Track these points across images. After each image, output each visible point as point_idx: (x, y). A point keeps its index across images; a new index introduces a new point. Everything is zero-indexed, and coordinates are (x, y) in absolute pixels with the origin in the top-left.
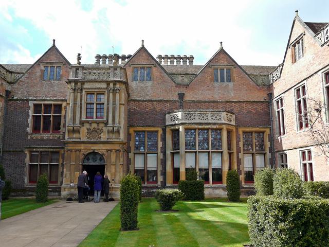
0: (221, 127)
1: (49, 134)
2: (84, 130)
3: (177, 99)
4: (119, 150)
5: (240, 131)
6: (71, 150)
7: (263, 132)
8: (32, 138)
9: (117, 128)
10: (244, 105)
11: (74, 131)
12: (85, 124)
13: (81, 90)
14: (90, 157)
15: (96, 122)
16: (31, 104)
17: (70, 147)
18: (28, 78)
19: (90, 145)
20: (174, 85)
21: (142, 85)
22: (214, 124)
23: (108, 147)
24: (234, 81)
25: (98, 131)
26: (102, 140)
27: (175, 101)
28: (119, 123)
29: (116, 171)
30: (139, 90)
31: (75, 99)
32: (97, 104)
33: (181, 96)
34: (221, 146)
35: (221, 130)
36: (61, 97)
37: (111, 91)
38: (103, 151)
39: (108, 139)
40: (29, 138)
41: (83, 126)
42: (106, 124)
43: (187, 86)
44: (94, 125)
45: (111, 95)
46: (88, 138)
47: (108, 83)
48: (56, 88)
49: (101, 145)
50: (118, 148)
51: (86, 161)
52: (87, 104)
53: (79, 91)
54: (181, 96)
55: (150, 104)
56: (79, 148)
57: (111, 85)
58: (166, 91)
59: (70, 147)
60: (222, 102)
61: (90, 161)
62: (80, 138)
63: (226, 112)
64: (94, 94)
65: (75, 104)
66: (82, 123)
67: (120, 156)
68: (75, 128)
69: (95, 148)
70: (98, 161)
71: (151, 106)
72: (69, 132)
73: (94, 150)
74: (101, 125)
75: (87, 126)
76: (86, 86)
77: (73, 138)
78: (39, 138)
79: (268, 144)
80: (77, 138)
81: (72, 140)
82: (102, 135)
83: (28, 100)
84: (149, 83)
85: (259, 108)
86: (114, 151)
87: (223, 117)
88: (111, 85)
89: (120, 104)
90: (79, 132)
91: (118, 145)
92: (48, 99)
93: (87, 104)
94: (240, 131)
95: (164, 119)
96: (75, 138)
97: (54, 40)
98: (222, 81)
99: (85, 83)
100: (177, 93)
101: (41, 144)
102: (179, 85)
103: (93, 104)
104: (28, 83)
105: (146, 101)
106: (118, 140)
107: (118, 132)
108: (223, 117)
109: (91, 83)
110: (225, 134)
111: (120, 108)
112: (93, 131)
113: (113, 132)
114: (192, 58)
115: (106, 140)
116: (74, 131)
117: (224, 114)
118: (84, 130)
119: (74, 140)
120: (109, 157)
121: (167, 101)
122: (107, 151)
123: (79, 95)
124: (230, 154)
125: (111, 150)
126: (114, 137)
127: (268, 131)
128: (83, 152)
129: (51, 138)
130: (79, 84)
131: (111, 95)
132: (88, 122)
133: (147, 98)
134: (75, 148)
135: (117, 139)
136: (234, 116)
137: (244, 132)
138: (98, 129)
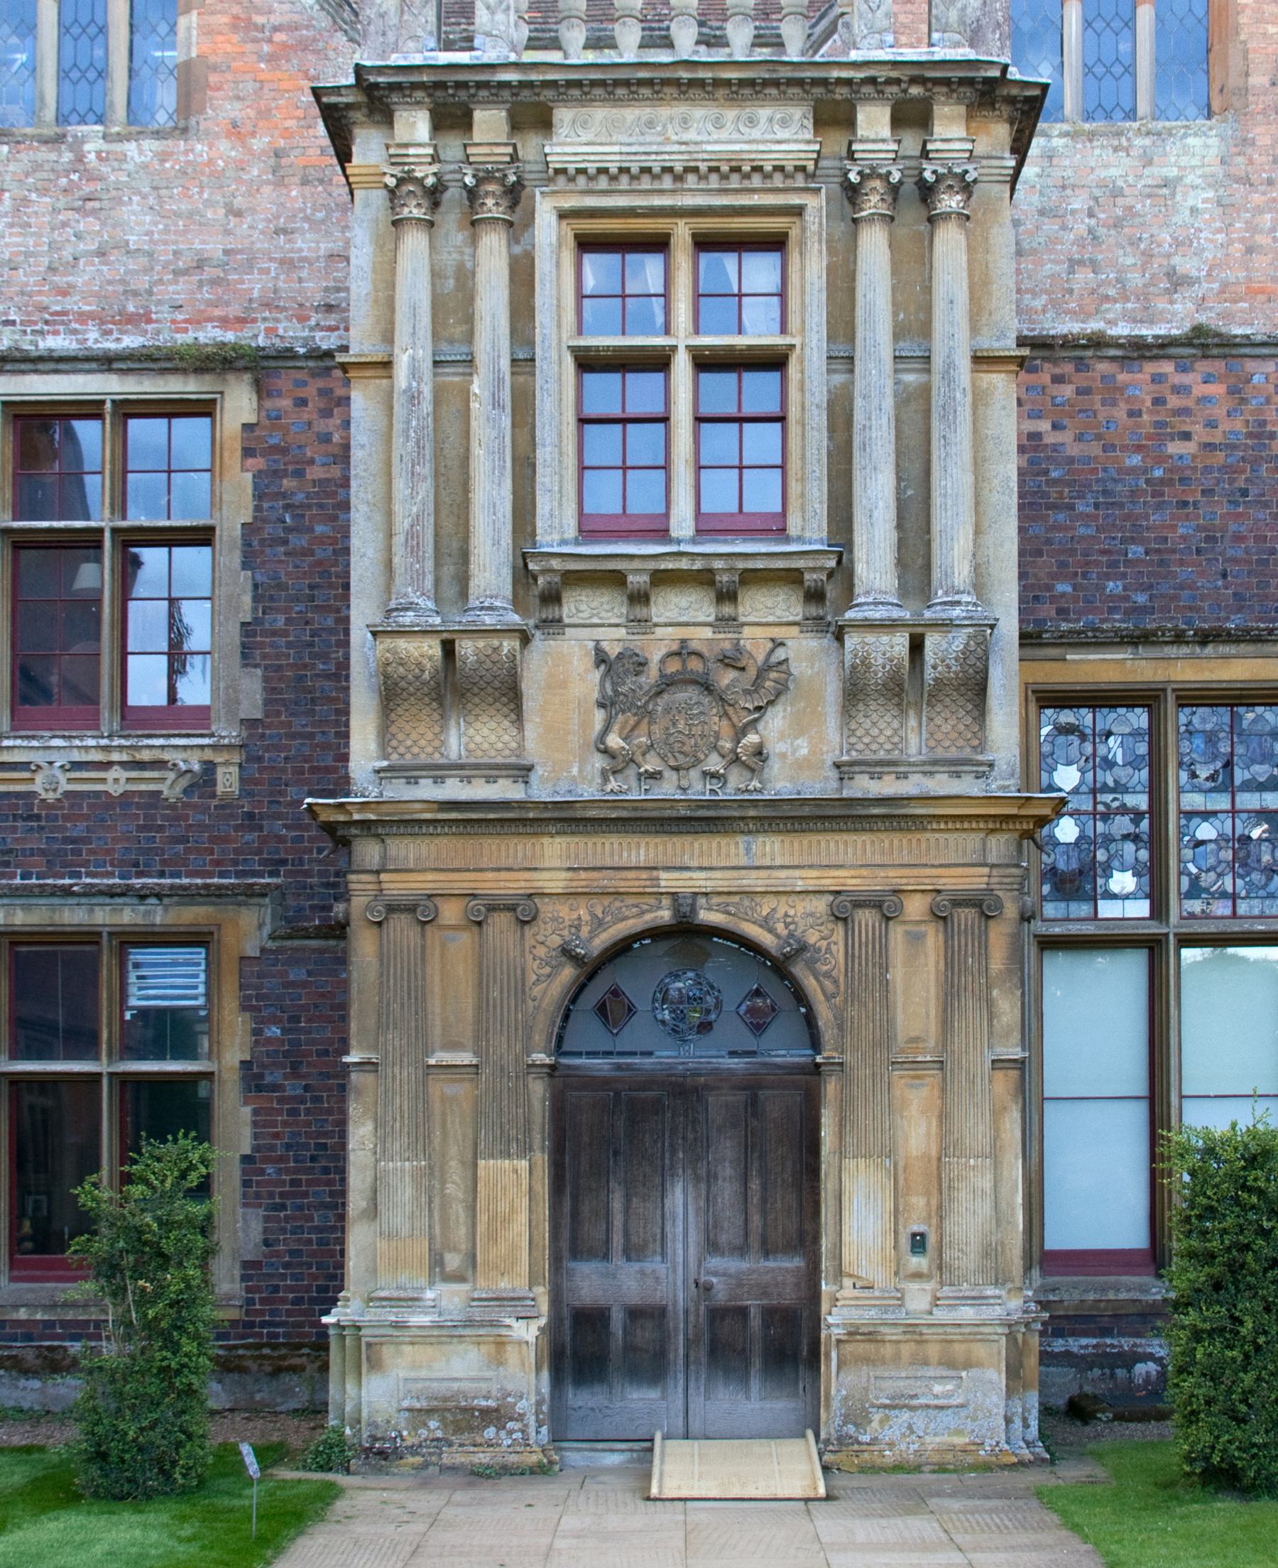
1: (88, 746)
2: (563, 672)
4: (982, 906)
6: (419, 911)
9: (958, 641)
12: (580, 606)
13: (515, 194)
14: (637, 983)
15: (704, 578)
17: (414, 868)
19: (640, 849)
23: (852, 861)
25: (722, 685)
26: (780, 783)
28: (979, 586)
29: (947, 1146)
30: (1081, 227)
31: (454, 305)
32: (706, 362)
36: (198, 321)
37: (873, 203)
38: (802, 907)
39: (844, 770)
41: (553, 625)
42: (815, 596)
44: (683, 615)
45: (874, 247)
46: (617, 763)
48: (137, 221)
49: (771, 847)
50: (974, 880)
51: (587, 1031)
52: (588, 362)
53: (492, 207)
55: (1202, 383)
56: (512, 884)
57: (874, 122)
59: (414, 868)
61: (639, 1033)
62: (523, 772)
64: (659, 244)
65: (453, 362)
66: (543, 590)
67: (997, 962)
68: (467, 649)
69: (705, 873)
70: (731, 1031)
71: (1219, 412)
72: (392, 694)
73: (683, 904)
74: (769, 610)
75: (595, 618)
76: (582, 136)
77: (439, 771)
80: (491, 771)
81: (427, 790)
82: (775, 724)
84: (1196, 150)
86: (915, 907)
89: (981, 360)
90: (508, 693)
91: (965, 844)
93: (588, 362)
96: (465, 770)
99: (563, 115)
103: (658, 362)
105: (1162, 348)
106: (968, 786)
107: (975, 689)
109: (631, 114)
111: (980, 399)
112: (668, 683)
113: (906, 686)
115: (821, 785)
116: (464, 682)
118: (563, 672)
119: (454, 790)
120: (870, 976)
122: (844, 908)
123: (493, 253)
125: (885, 906)
126: (914, 746)
128: (566, 922)
129: (116, 782)
130: (489, 122)
131: (874, 247)
133: (1175, 319)
134: (463, 883)
135: (955, 766)
138: (730, 661)
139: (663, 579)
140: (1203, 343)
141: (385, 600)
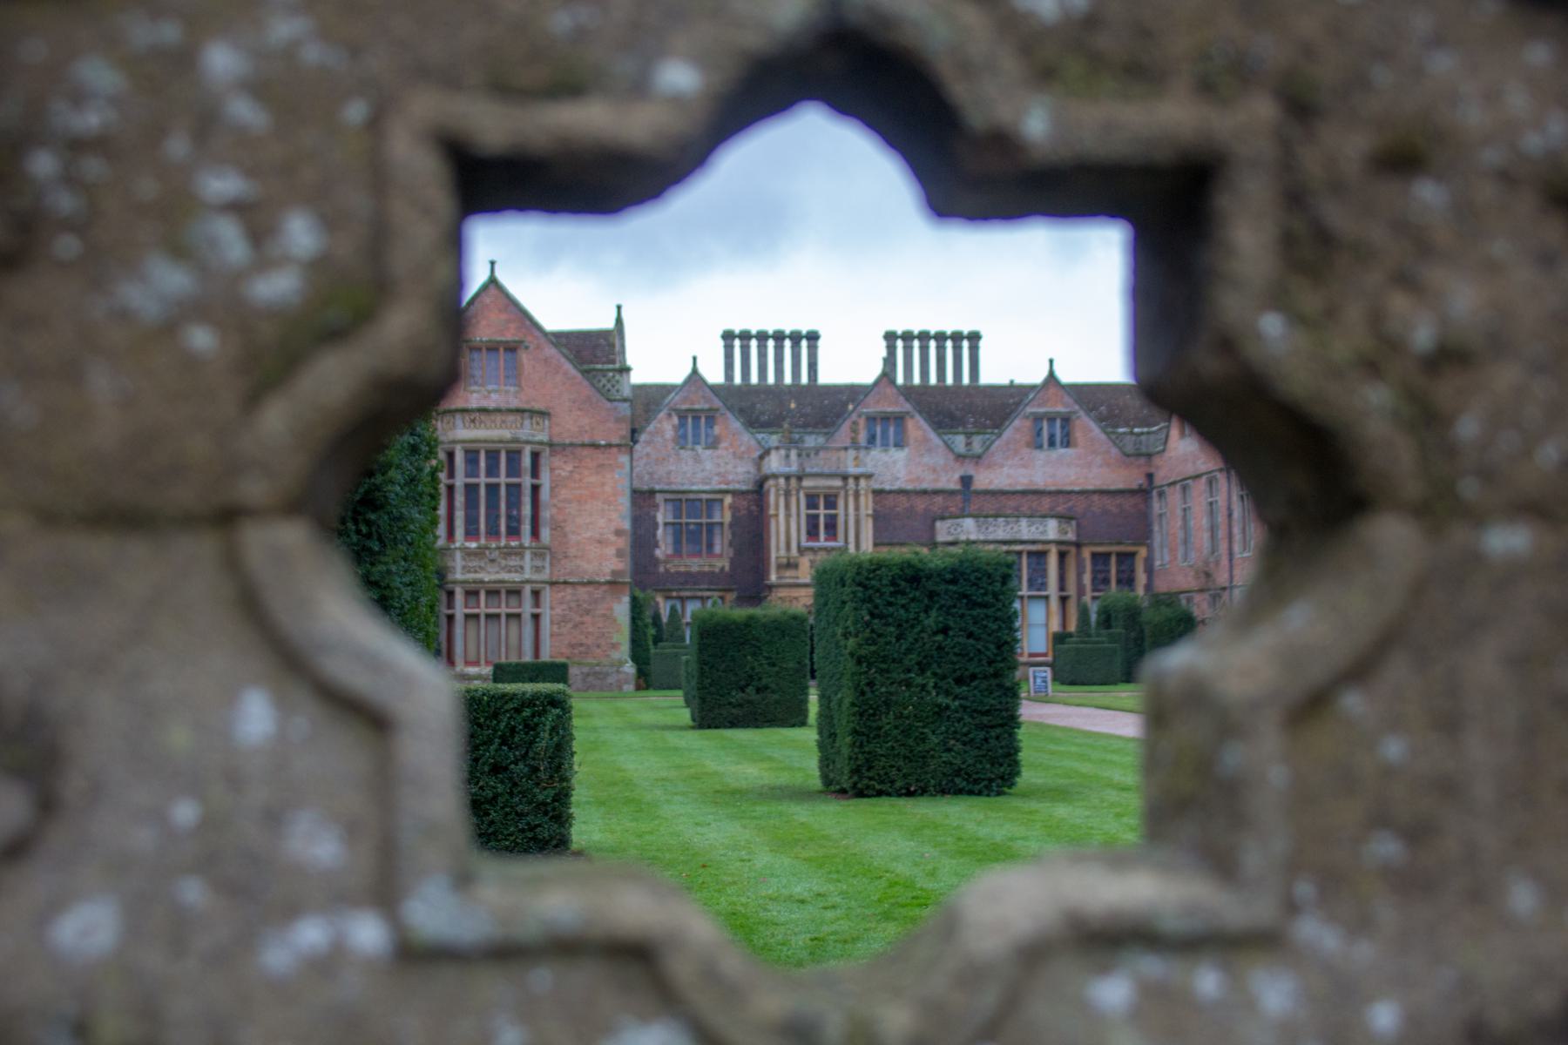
0: (1046, 547)
2: (805, 562)
3: (958, 487)
5: (1086, 553)
7: (1132, 555)
8: (667, 571)
10: (1096, 498)
11: (791, 565)
15: (825, 549)
16: (659, 498)
17: (783, 593)
18: (648, 443)
20: (951, 457)
21: (884, 457)
22: (1034, 542)
24: (1075, 446)
27: (952, 493)
33: (966, 481)
34: (1044, 586)
35: (1042, 555)
40: (662, 569)
43: (978, 458)
47: (845, 478)
48: (709, 466)
54: (966, 481)
55: (903, 499)
57: (851, 481)
58: (934, 470)
60: (1050, 493)
63: (1059, 517)
72: (779, 567)
76: (806, 483)
78: (682, 569)
79: (1141, 578)
83: (652, 492)
84: (899, 455)
85: (1128, 503)
88: (851, 481)
90: (795, 566)
92: (694, 488)
94: (1086, 553)
97: (695, 359)
98: (1052, 444)
100: (957, 476)
101: (686, 582)
102: (960, 457)
104: (648, 455)
114: (974, 337)
116: (791, 565)
118: (805, 562)
121: (936, 492)
124: (1064, 600)
127: (1143, 552)
129: (706, 569)
130: (793, 482)
132: (811, 549)
136: (1074, 523)
137: (1094, 555)
139: (821, 549)
140: (902, 492)
141: (776, 551)
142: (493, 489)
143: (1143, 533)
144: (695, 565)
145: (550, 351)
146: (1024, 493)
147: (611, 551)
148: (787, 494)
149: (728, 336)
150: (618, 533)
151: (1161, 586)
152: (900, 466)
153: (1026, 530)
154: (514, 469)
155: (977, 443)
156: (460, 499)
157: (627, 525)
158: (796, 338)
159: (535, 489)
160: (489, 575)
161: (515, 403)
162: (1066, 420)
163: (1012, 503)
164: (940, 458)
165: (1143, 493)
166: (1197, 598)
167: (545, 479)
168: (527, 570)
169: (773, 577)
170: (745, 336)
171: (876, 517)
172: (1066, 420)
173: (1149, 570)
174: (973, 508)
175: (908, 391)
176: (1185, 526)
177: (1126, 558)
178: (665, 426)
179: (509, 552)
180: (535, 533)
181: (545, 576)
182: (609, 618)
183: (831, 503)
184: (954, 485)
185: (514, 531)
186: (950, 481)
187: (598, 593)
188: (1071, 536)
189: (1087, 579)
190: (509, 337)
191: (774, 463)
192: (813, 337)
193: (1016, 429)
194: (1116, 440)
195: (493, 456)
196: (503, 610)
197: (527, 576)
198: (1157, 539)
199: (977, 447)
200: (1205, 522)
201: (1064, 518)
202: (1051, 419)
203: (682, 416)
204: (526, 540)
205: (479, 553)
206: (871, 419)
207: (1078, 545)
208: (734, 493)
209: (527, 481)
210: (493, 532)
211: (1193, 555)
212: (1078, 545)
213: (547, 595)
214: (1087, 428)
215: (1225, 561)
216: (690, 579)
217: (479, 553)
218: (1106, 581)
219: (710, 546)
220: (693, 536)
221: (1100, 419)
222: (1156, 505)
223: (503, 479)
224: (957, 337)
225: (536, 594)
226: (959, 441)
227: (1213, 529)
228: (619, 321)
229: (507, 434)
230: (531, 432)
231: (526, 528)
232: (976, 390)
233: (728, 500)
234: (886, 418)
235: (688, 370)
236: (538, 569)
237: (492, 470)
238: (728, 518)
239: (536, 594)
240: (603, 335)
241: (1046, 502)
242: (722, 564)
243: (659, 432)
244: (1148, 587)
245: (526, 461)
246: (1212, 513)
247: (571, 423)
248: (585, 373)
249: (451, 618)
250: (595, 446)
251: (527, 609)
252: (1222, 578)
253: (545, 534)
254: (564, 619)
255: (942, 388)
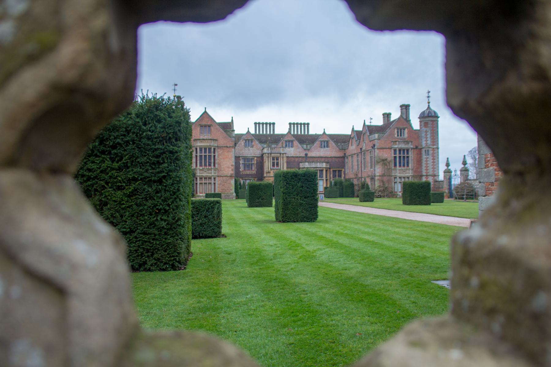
2: (272, 172)
5: (331, 170)
11: (269, 172)
16: (241, 158)
17: (267, 178)
33: (306, 155)
34: (322, 177)
35: (322, 170)
43: (309, 150)
47: (280, 154)
54: (306, 155)
63: (326, 162)
72: (266, 173)
76: (272, 155)
79: (343, 175)
83: (239, 157)
84: (292, 149)
85: (340, 160)
87: (324, 165)
90: (270, 173)
94: (331, 170)
95: (299, 165)
98: (324, 147)
102: (305, 150)
108: (324, 165)
110: (324, 172)
114: (308, 124)
116: (269, 172)
117: (324, 164)
118: (272, 172)
121: (300, 157)
124: (327, 180)
127: (343, 170)
137: (333, 171)
140: (292, 157)
142: (205, 156)
143: (344, 167)
144: (248, 172)
145: (218, 127)
146: (319, 157)
147: (230, 169)
148: (268, 157)
149: (255, 124)
150: (232, 165)
151: (347, 177)
152: (291, 151)
153: (319, 165)
154: (210, 152)
155: (309, 146)
156: (198, 158)
157: (234, 164)
158: (270, 124)
159: (214, 156)
160: (205, 174)
161: (210, 138)
162: (327, 142)
163: (316, 159)
164: (301, 150)
165: (344, 157)
166: (354, 180)
167: (216, 154)
168: (213, 173)
169: (265, 175)
170: (259, 124)
171: (287, 162)
172: (327, 142)
173: (345, 174)
174: (308, 160)
175: (294, 136)
176: (352, 164)
177: (340, 171)
178: (242, 143)
179: (209, 170)
180: (214, 166)
181: (216, 175)
182: (230, 183)
183: (277, 159)
184: (304, 156)
185: (210, 165)
186: (303, 155)
187: (228, 178)
188: (328, 166)
189: (332, 176)
190: (209, 124)
191: (265, 151)
192: (274, 124)
193: (317, 143)
194: (338, 146)
195: (205, 149)
196: (208, 182)
197: (213, 174)
198: (346, 167)
199: (309, 147)
200: (356, 164)
201: (327, 163)
202: (324, 142)
203: (246, 141)
204: (212, 167)
205: (203, 170)
206: (286, 141)
207: (330, 168)
208: (257, 157)
209: (212, 154)
210: (205, 165)
211: (354, 171)
212: (330, 168)
213: (217, 179)
214: (332, 143)
215: (360, 172)
216: (248, 175)
217: (203, 170)
218: (336, 176)
219: (252, 168)
220: (248, 166)
221: (334, 142)
222: (346, 160)
223: (207, 154)
224: (304, 124)
225: (215, 178)
226: (305, 146)
227: (358, 165)
228: (232, 120)
229: (208, 144)
230: (213, 144)
231: (212, 164)
232: (308, 135)
233: (255, 158)
234: (289, 141)
235: (247, 131)
236: (215, 173)
237: (205, 152)
238: (255, 162)
239: (215, 178)
240: (229, 123)
241: (323, 159)
242: (254, 172)
243: (241, 144)
244: (344, 177)
245: (212, 150)
246: (358, 162)
247: (222, 142)
248: (225, 131)
249: (197, 184)
250: (227, 147)
251: (213, 182)
252: (360, 176)
253: (216, 165)
254: (220, 184)
255: (301, 135)
